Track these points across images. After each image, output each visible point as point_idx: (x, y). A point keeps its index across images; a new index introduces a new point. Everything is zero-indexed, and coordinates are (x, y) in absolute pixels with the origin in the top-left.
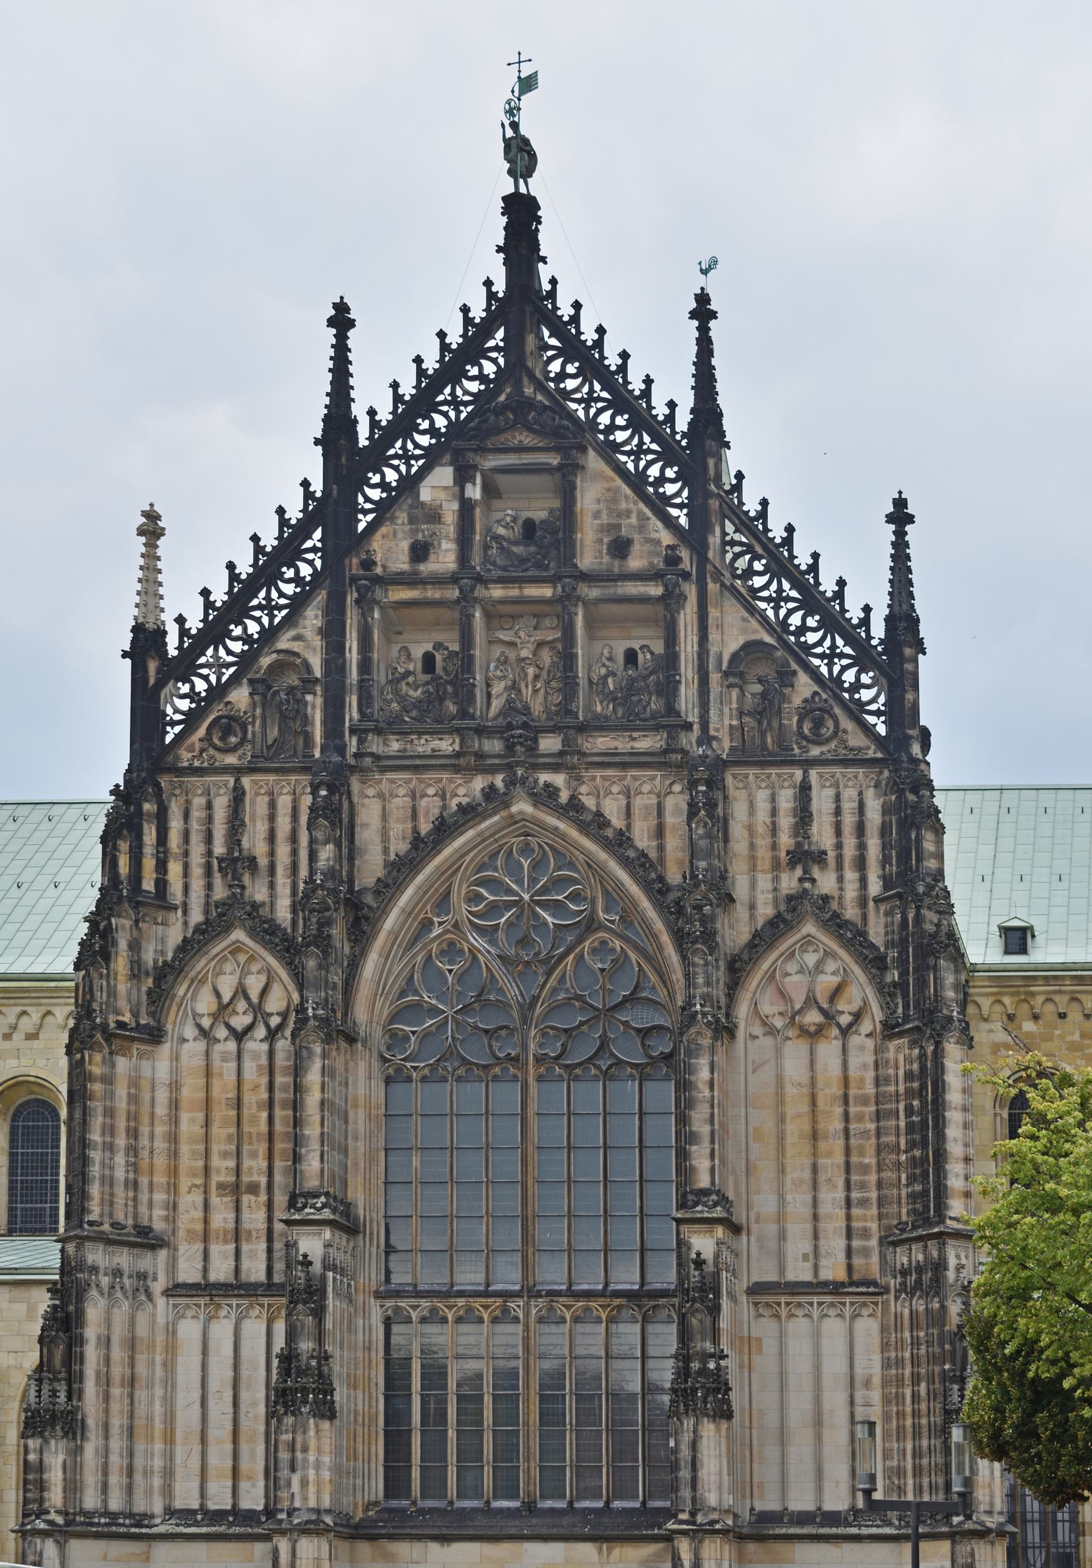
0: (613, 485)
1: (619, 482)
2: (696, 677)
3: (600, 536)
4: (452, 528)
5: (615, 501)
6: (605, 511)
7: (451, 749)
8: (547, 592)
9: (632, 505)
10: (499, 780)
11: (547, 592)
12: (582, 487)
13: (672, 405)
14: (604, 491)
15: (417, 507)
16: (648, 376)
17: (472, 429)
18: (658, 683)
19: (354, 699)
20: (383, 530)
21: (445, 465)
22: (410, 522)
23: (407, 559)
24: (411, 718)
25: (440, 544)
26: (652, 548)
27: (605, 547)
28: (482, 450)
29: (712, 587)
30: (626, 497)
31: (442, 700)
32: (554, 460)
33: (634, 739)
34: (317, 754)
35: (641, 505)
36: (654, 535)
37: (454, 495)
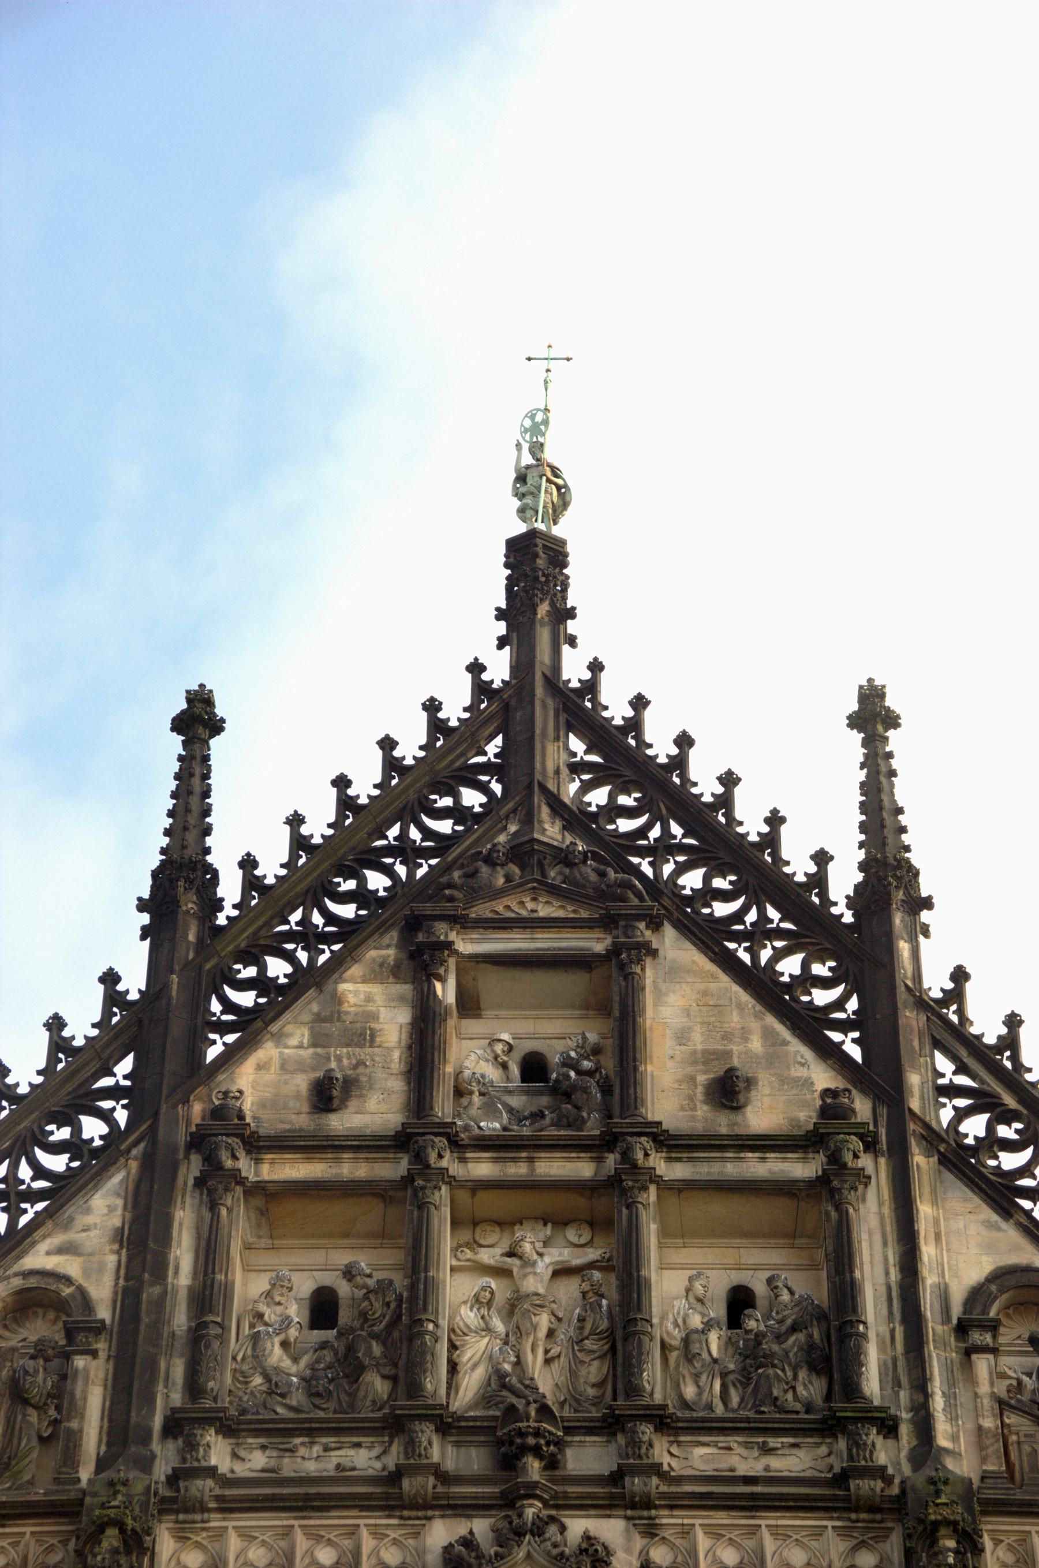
1: (724, 981)
3: (689, 1070)
4: (396, 1055)
7: (378, 1465)
8: (583, 1169)
10: (481, 1527)
11: (583, 1169)
13: (822, 858)
16: (775, 812)
18: (810, 1347)
19: (178, 1369)
22: (314, 1045)
24: (290, 1408)
27: (700, 1089)
28: (461, 922)
29: (920, 1160)
31: (361, 1369)
32: (597, 943)
34: (85, 1474)
35: (771, 1020)
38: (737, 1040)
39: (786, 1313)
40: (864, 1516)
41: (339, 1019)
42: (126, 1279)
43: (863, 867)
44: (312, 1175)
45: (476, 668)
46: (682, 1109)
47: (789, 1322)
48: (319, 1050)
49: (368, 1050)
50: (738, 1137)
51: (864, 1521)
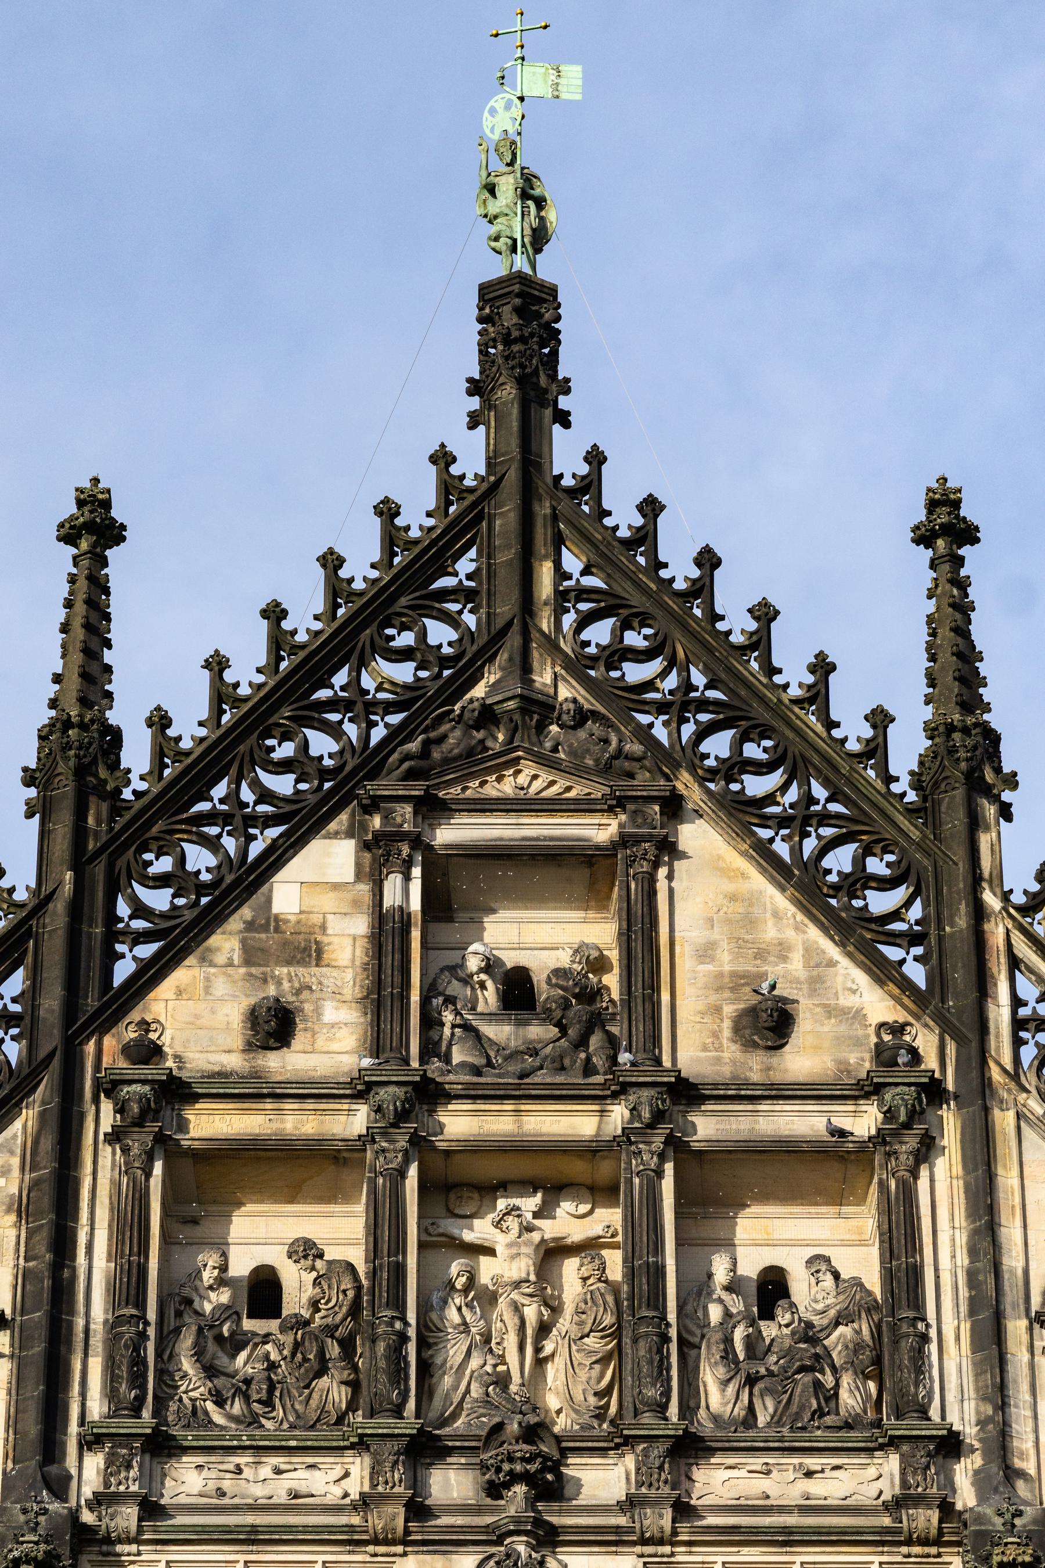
0: (742, 887)
2: (966, 1327)
3: (713, 998)
4: (349, 975)
5: (750, 922)
6: (725, 945)
7: (337, 1491)
9: (790, 934)
12: (671, 891)
13: (880, 719)
14: (721, 900)
15: (265, 928)
16: (821, 656)
17: (407, 757)
20: (180, 976)
21: (336, 835)
22: (248, 962)
23: (237, 1041)
24: (231, 1417)
25: (318, 1012)
26: (843, 1028)
27: (727, 1024)
30: (776, 915)
33: (809, 1474)
35: (814, 933)
36: (847, 1001)
37: (356, 903)
38: (772, 959)
39: (828, 1302)
40: (917, 1550)
41: (277, 930)
42: (26, 1260)
43: (931, 730)
44: (249, 1131)
45: (443, 458)
46: (705, 1049)
47: (832, 1313)
48: (254, 970)
49: (314, 970)
50: (772, 1086)
51: (916, 1556)
